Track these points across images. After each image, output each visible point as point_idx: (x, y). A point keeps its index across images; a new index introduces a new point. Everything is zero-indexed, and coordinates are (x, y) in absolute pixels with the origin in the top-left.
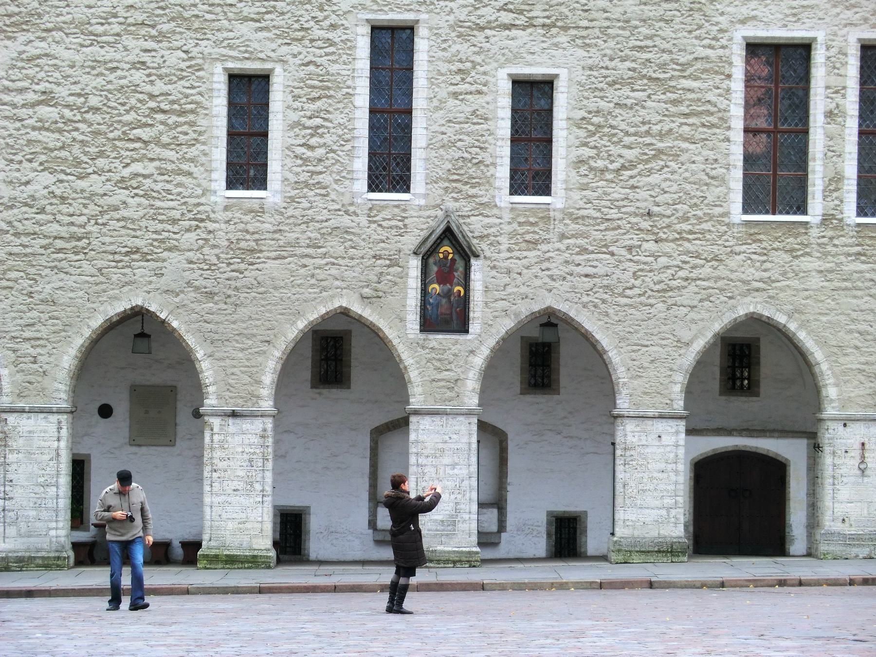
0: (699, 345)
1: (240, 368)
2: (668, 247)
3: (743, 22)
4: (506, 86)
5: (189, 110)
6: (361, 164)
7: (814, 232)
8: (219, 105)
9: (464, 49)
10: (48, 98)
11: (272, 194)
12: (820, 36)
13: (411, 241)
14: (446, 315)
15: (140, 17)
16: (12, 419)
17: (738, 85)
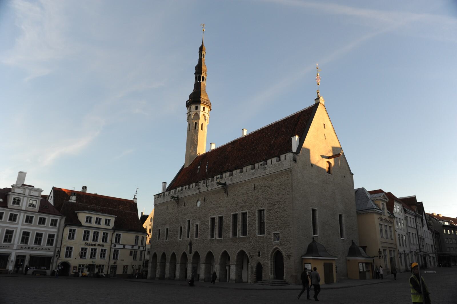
0: (206, 255)
1: (179, 259)
2: (204, 243)
3: (210, 216)
4: (195, 226)
5: (177, 231)
6: (186, 235)
7: (214, 240)
8: (179, 230)
9: (193, 222)
10: (171, 231)
11: (181, 240)
12: (215, 216)
13: (188, 244)
14: (190, 252)
15: (175, 222)
16: (167, 264)
17: (210, 223)
